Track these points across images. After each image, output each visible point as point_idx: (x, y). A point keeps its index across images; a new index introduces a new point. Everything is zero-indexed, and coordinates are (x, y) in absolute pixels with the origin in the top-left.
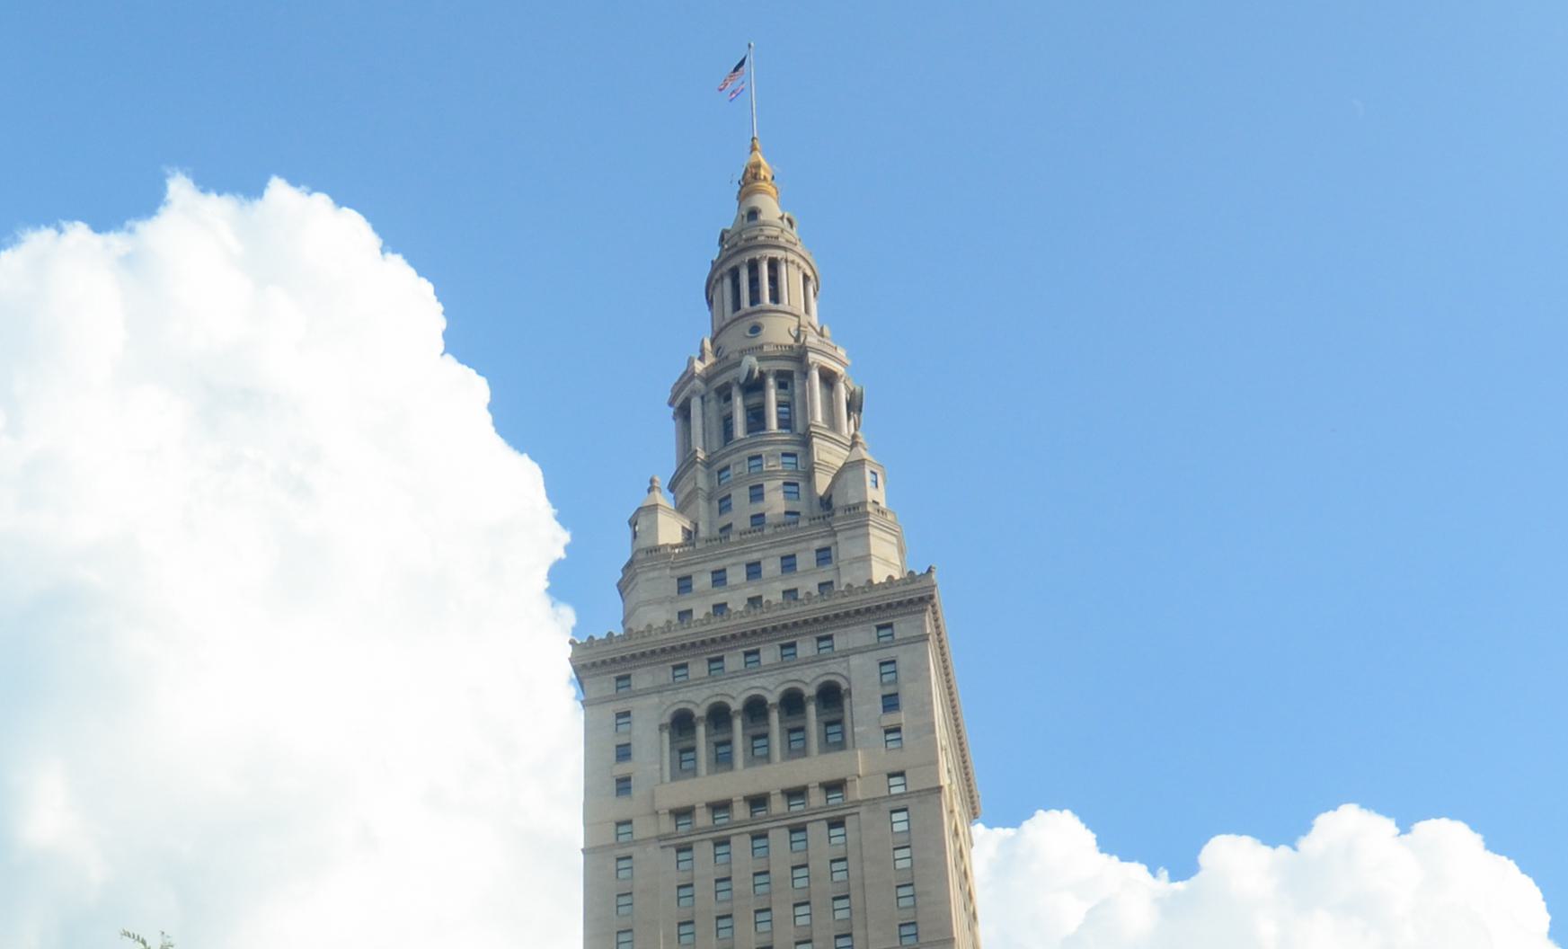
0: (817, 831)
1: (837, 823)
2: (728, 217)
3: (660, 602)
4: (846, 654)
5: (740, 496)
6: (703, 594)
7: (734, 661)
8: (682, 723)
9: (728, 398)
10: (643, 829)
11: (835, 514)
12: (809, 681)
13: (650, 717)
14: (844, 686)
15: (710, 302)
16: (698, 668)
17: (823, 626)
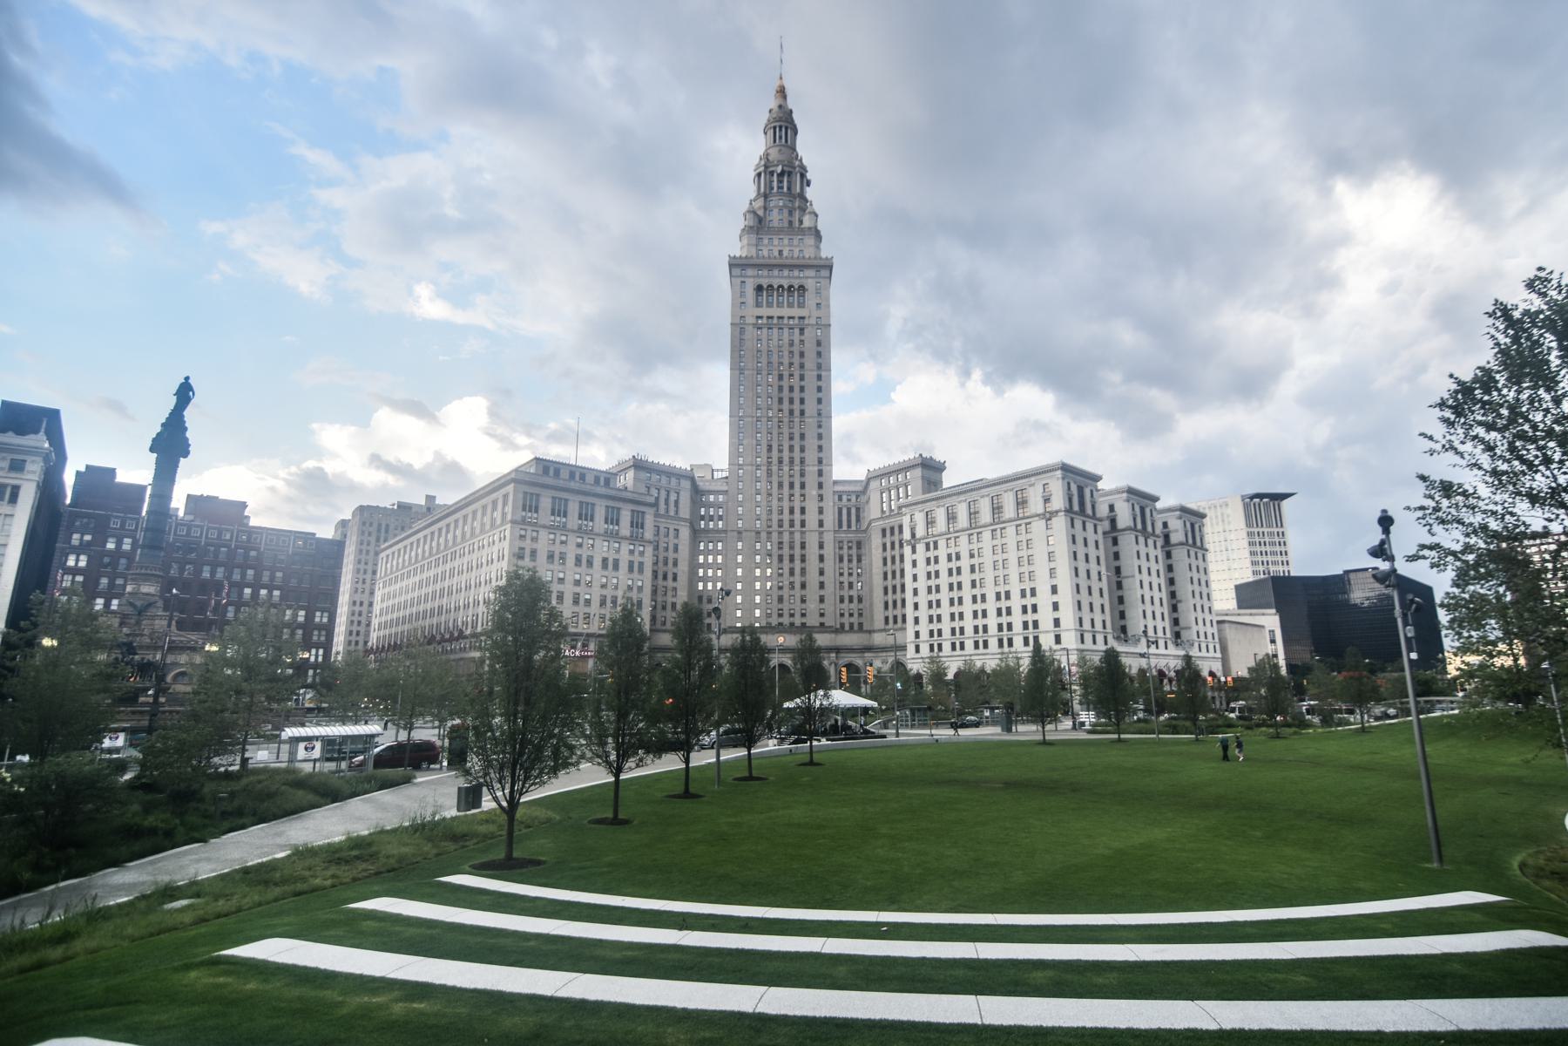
1: (802, 330)
2: (773, 103)
8: (759, 288)
12: (796, 283)
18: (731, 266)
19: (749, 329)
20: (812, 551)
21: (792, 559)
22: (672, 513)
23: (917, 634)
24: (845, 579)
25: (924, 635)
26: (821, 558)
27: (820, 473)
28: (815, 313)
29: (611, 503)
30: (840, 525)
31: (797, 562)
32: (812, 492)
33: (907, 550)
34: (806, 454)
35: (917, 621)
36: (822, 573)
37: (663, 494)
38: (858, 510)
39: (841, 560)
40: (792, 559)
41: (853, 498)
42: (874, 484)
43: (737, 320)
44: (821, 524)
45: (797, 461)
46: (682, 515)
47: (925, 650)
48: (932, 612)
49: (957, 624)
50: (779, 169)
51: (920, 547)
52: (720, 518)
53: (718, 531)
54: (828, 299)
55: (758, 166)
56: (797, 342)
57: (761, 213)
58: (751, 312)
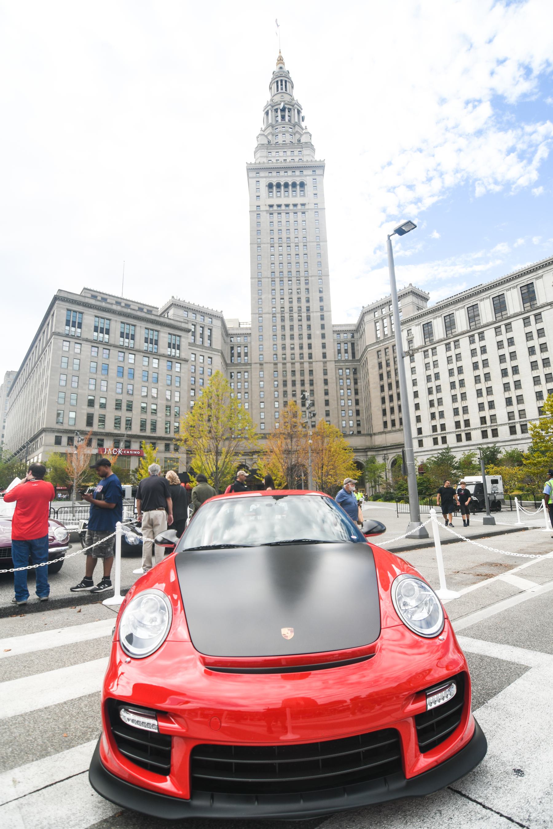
0: (299, 214)
1: (304, 213)
3: (265, 157)
4: (306, 176)
5: (280, 135)
6: (274, 157)
7: (282, 173)
8: (270, 186)
9: (277, 112)
10: (263, 208)
12: (298, 181)
13: (263, 183)
14: (305, 183)
15: (270, 88)
16: (274, 174)
17: (301, 168)
18: (249, 170)
20: (319, 377)
21: (303, 383)
22: (207, 343)
23: (420, 431)
25: (427, 430)
26: (326, 382)
27: (322, 318)
29: (150, 326)
31: (307, 387)
32: (316, 332)
33: (407, 359)
34: (311, 304)
36: (326, 393)
37: (199, 330)
38: (353, 344)
40: (303, 383)
41: (350, 336)
42: (367, 318)
43: (255, 208)
44: (324, 356)
46: (214, 346)
47: (428, 443)
48: (433, 410)
49: (461, 418)
50: (281, 106)
51: (419, 356)
52: (246, 354)
53: (246, 364)
54: (322, 190)
55: (266, 107)
57: (270, 137)
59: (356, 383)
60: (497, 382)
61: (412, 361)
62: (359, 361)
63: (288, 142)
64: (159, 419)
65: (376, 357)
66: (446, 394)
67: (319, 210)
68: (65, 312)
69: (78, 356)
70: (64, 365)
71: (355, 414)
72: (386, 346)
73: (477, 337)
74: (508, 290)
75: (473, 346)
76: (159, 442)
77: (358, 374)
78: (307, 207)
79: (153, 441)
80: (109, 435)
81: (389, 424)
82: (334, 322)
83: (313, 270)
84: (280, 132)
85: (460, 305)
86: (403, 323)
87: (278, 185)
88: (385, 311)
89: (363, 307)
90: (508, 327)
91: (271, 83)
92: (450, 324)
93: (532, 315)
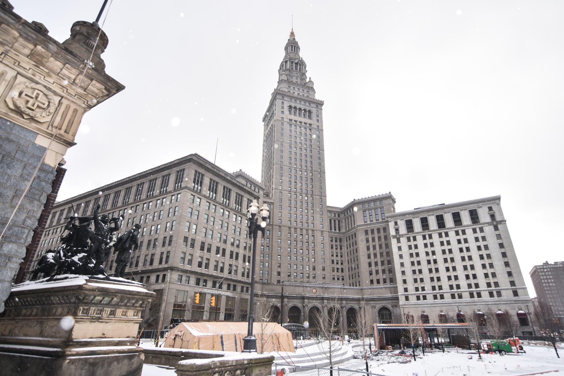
0: (308, 129)
1: (310, 129)
5: (294, 78)
7: (298, 102)
8: (290, 107)
10: (285, 120)
11: (309, 87)
16: (293, 100)
19: (285, 124)
23: (406, 290)
24: (334, 258)
25: (411, 290)
28: (318, 124)
30: (331, 229)
35: (405, 282)
38: (339, 221)
39: (332, 248)
41: (337, 215)
43: (280, 119)
45: (310, 192)
50: (296, 61)
51: (403, 240)
54: (322, 119)
56: (308, 134)
58: (287, 115)
59: (341, 249)
60: (459, 264)
61: (399, 241)
62: (344, 233)
63: (299, 83)
64: (239, 266)
65: (364, 234)
66: (425, 267)
67: (320, 130)
68: (194, 172)
69: (198, 209)
70: (189, 215)
71: (340, 271)
72: (372, 228)
73: (443, 235)
74: (462, 210)
75: (441, 240)
76: (238, 284)
77: (343, 243)
78: (313, 126)
79: (235, 283)
80: (211, 276)
81: (375, 281)
82: (328, 204)
83: (316, 167)
84: (295, 76)
85: (431, 213)
86: (391, 217)
87: (295, 108)
88: (372, 204)
89: (354, 200)
90: (464, 232)
91: (287, 45)
92: (425, 223)
93: (477, 227)
